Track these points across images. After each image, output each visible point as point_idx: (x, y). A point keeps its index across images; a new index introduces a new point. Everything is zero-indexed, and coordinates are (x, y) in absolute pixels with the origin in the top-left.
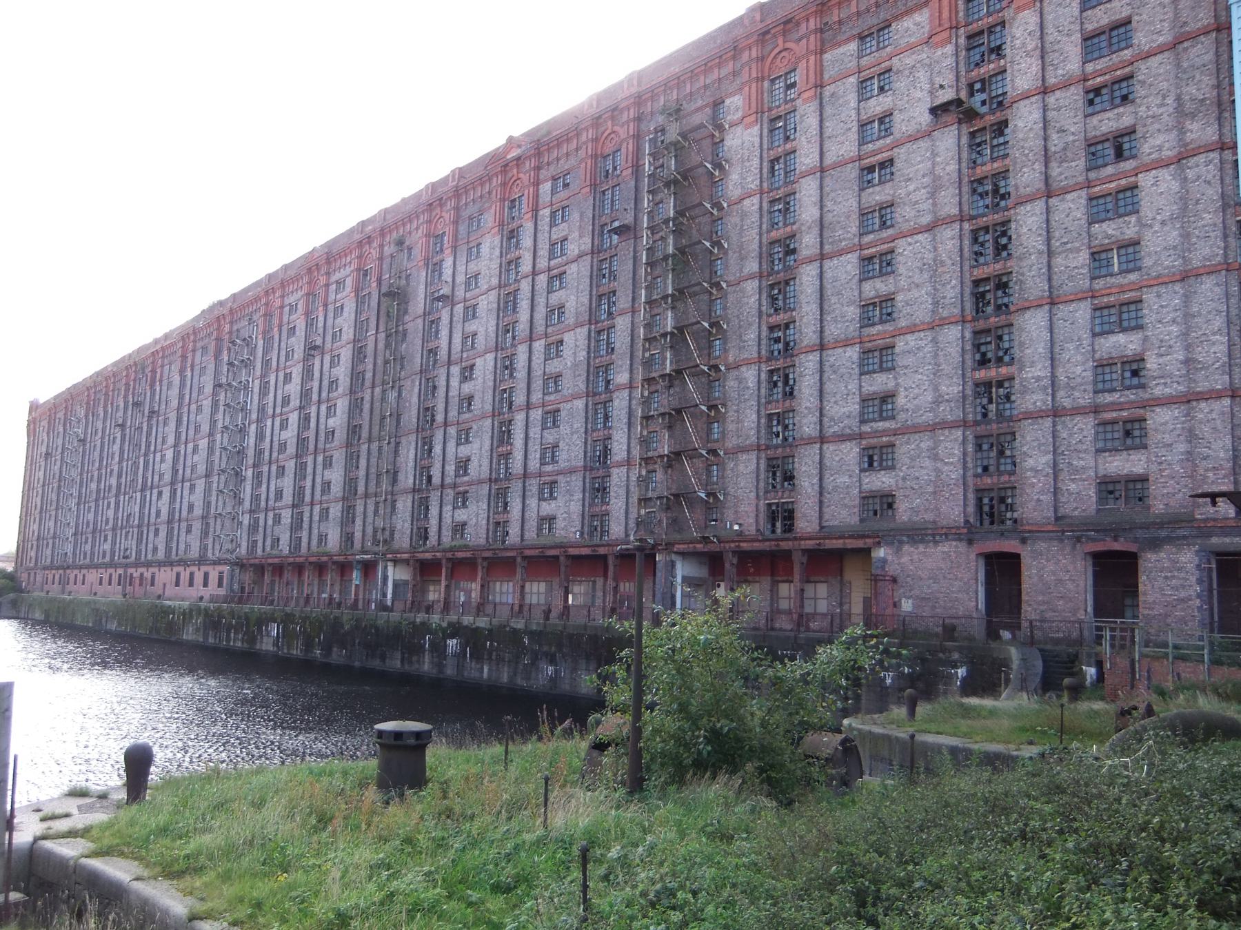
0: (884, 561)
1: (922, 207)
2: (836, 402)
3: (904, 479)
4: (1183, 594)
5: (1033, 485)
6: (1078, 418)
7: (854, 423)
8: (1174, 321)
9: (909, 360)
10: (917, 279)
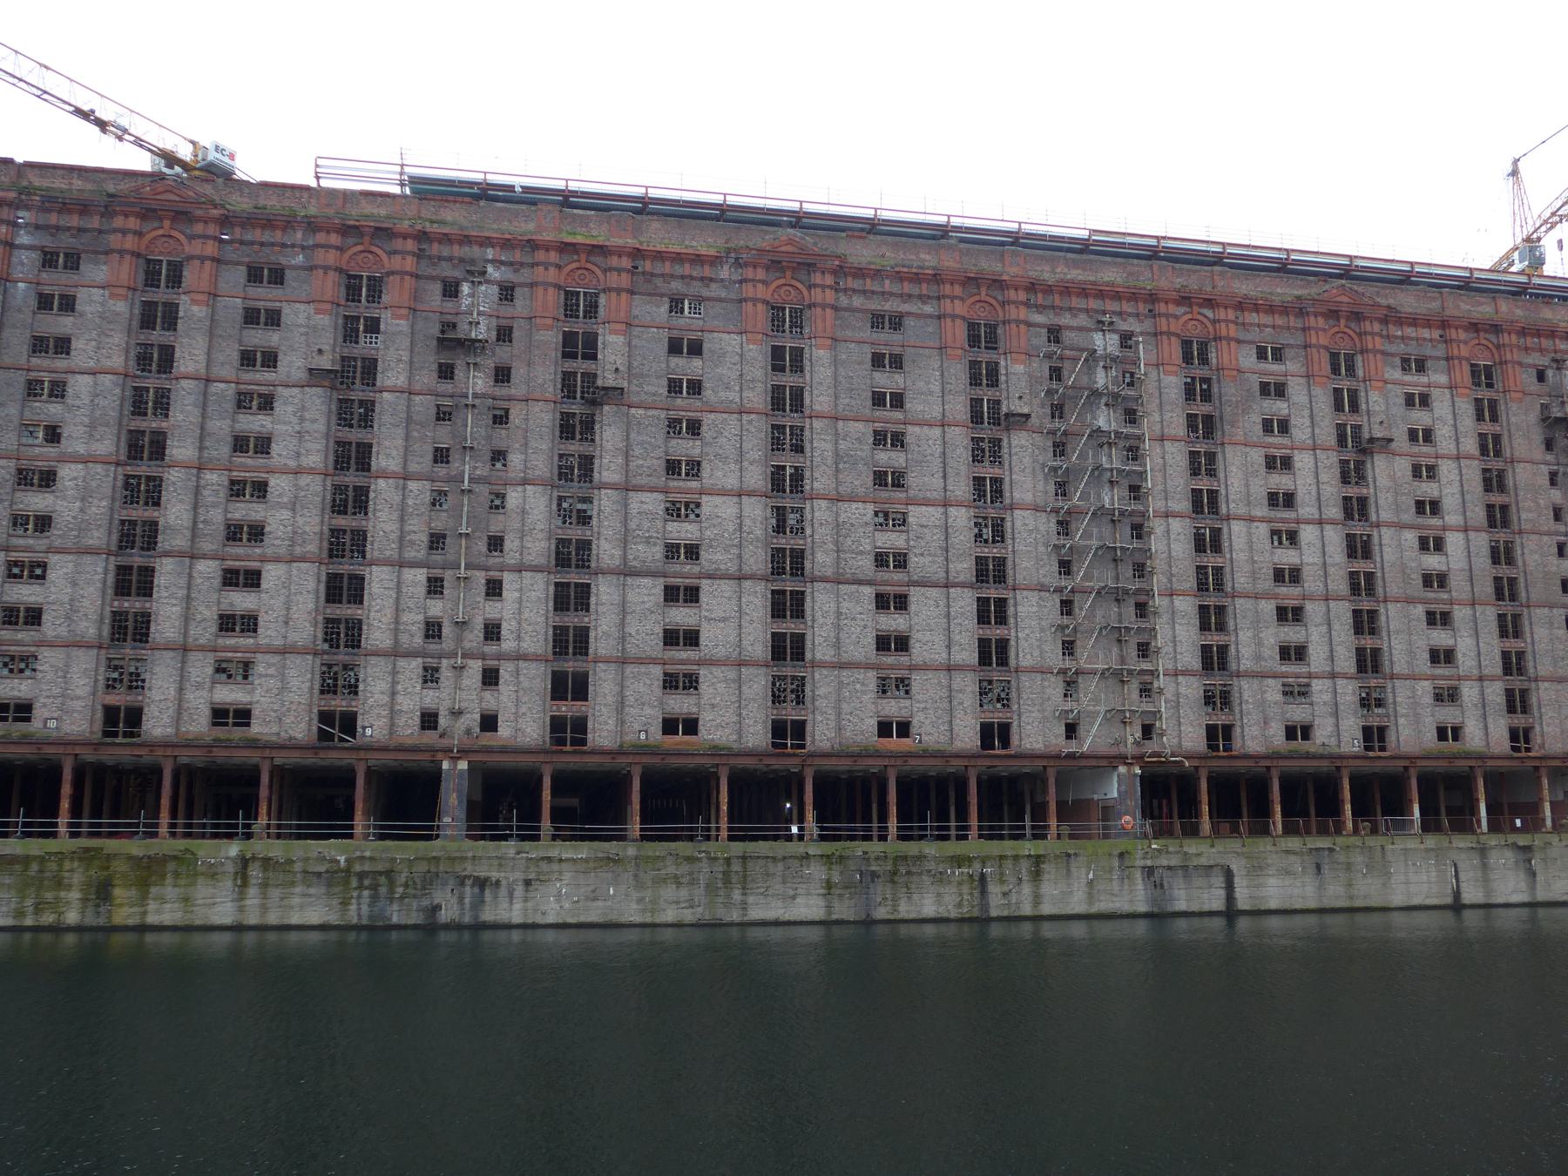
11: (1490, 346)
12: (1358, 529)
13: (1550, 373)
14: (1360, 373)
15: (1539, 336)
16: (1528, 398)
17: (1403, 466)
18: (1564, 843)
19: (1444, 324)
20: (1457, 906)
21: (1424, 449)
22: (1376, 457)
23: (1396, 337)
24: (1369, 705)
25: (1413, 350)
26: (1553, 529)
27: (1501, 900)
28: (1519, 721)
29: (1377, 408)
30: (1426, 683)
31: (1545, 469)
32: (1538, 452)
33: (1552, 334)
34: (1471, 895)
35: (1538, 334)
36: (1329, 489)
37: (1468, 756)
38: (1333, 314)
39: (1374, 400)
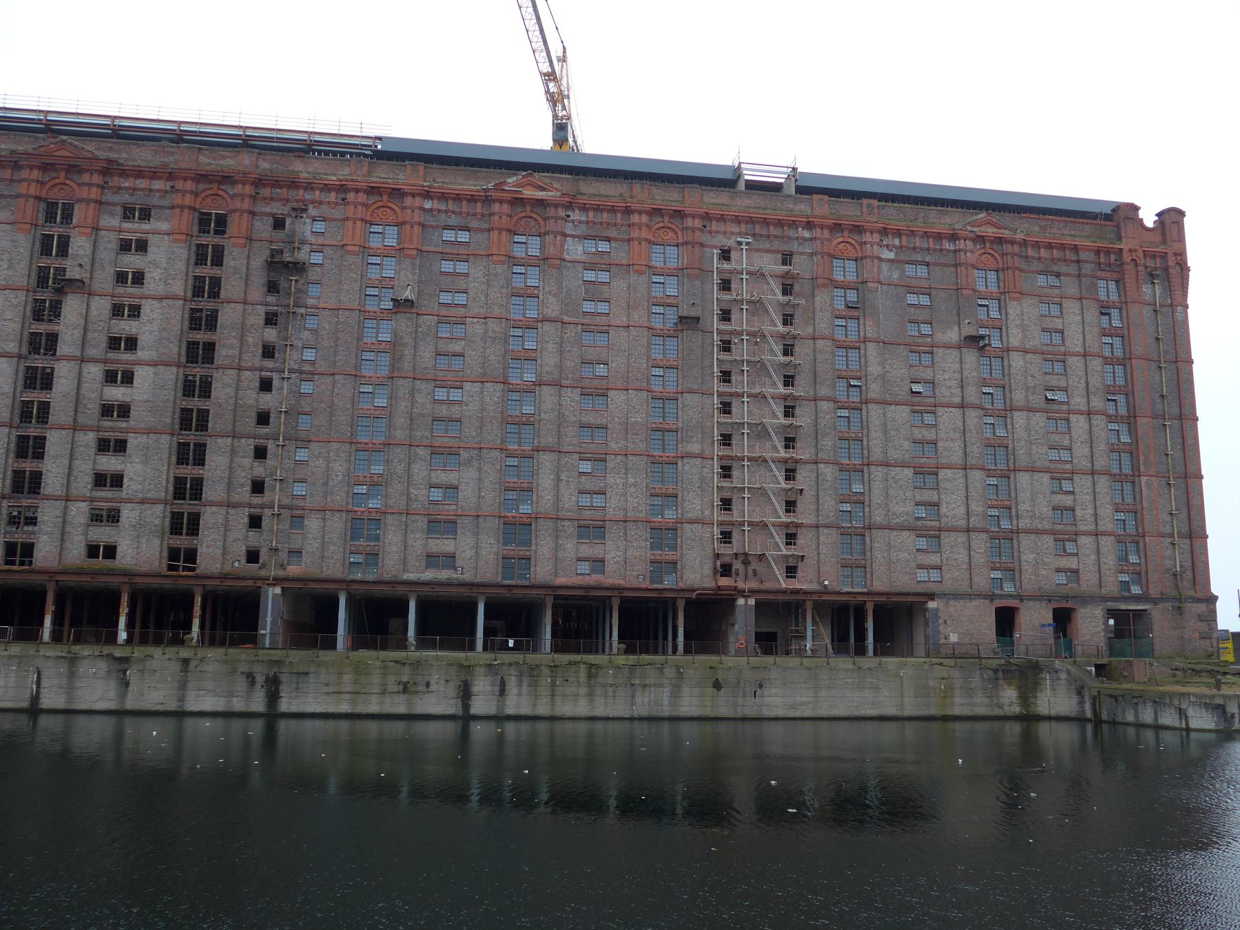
0: (937, 610)
1: (954, 391)
2: (897, 503)
3: (947, 559)
4: (1097, 630)
5: (1027, 570)
6: (1045, 536)
7: (911, 520)
8: (1088, 493)
9: (949, 485)
10: (951, 435)
11: (226, 196)
12: (39, 362)
13: (288, 221)
14: (75, 221)
15: (281, 187)
16: (256, 244)
17: (101, 307)
18: (167, 656)
19: (171, 176)
20: (34, 710)
21: (130, 290)
22: (70, 296)
23: (119, 188)
24: (19, 523)
25: (138, 200)
26: (258, 365)
27: (83, 707)
28: (182, 542)
29: (81, 252)
30: (83, 504)
31: (261, 310)
32: (257, 292)
33: (293, 184)
34: (51, 699)
35: (276, 184)
36: (11, 325)
37: (112, 573)
38: (46, 167)
39: (80, 245)
